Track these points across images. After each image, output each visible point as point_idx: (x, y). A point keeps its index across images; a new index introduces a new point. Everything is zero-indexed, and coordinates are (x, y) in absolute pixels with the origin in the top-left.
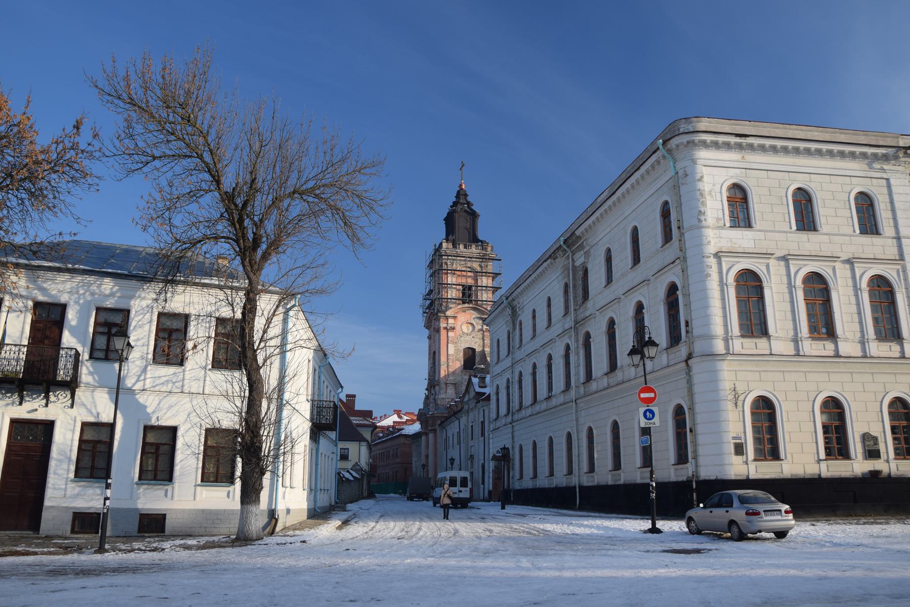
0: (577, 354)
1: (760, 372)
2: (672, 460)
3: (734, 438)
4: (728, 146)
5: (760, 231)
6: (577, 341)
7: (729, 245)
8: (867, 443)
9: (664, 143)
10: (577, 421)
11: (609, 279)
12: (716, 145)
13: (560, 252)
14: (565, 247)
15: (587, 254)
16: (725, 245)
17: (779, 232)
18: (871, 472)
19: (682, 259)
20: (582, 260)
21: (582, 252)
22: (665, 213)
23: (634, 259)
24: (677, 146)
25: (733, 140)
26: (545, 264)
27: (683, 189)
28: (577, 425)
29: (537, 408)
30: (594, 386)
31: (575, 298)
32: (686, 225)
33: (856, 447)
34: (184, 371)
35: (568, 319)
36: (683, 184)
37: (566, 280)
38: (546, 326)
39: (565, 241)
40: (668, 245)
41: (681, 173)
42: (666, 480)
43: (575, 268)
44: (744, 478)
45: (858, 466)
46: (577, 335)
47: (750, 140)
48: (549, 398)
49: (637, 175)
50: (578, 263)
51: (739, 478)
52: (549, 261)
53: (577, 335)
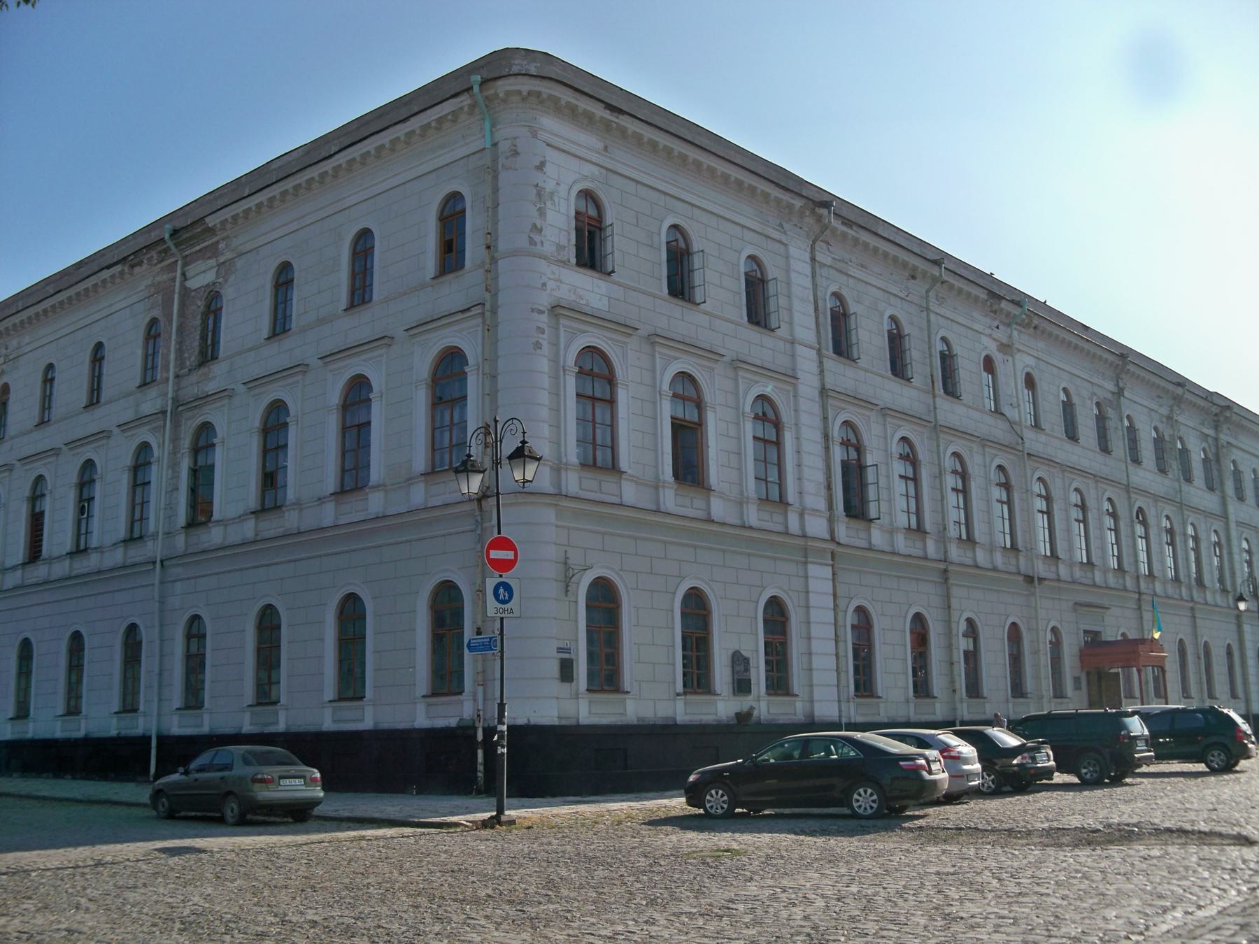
0: (174, 466)
1: (604, 534)
2: (330, 692)
3: (560, 650)
4: (588, 121)
5: (619, 284)
6: (175, 439)
7: (573, 297)
8: (738, 668)
9: (484, 83)
10: (162, 603)
11: (280, 326)
12: (572, 114)
13: (154, 253)
14: (170, 244)
15: (225, 268)
16: (564, 295)
17: (645, 293)
18: (738, 715)
19: (485, 310)
20: (210, 277)
21: (213, 262)
22: (452, 216)
23: (353, 292)
24: (508, 94)
25: (599, 112)
26: (106, 274)
27: (503, 176)
28: (161, 611)
29: (39, 572)
30: (215, 536)
31: (180, 351)
32: (502, 246)
33: (721, 674)
34: (564, 263)
35: (153, 392)
36: (506, 168)
37: (157, 313)
38: (84, 401)
39: (175, 233)
40: (450, 277)
41: (504, 147)
42: (401, 726)
43: (185, 292)
44: (573, 722)
45: (722, 706)
46: (176, 425)
47: (625, 121)
48: (79, 551)
49: (400, 131)
50: (193, 284)
51: (564, 722)
52: (118, 268)
53: (176, 425)
